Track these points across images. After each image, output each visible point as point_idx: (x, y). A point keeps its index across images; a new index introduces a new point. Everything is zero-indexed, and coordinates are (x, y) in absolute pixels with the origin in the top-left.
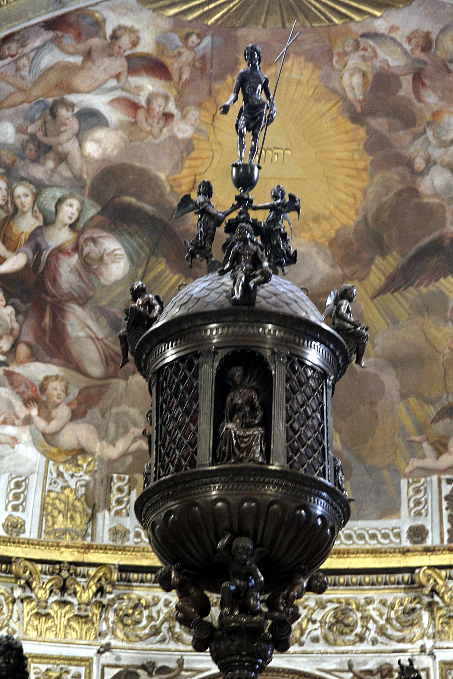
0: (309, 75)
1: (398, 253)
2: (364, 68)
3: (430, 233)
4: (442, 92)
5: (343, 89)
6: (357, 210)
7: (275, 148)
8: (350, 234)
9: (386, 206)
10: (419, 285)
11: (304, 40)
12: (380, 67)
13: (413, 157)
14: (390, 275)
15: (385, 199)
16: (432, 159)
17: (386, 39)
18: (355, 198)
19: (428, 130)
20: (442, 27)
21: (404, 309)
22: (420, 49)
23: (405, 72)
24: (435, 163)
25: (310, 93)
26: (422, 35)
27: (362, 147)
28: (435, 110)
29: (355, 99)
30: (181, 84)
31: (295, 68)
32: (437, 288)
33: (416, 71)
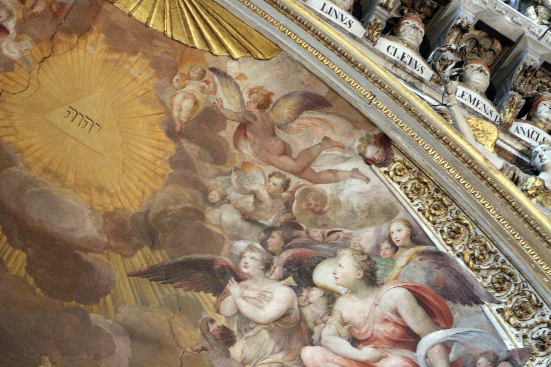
0: (146, 78)
1: (167, 253)
2: (198, 98)
3: (204, 253)
4: (259, 150)
5: (172, 105)
6: (141, 203)
7: (86, 117)
8: (128, 217)
9: (170, 213)
10: (180, 287)
11: (157, 46)
12: (214, 103)
13: (211, 188)
14: (153, 266)
15: (171, 207)
16: (228, 198)
17: (231, 82)
18: (143, 193)
19: (233, 174)
20: (286, 93)
21: (158, 298)
22: (257, 104)
23: (234, 118)
24: (229, 202)
25: (140, 93)
26: (265, 93)
27: (167, 158)
28: (246, 161)
29: (179, 119)
30: (30, 12)
31: (136, 67)
32: (195, 297)
33: (244, 121)
